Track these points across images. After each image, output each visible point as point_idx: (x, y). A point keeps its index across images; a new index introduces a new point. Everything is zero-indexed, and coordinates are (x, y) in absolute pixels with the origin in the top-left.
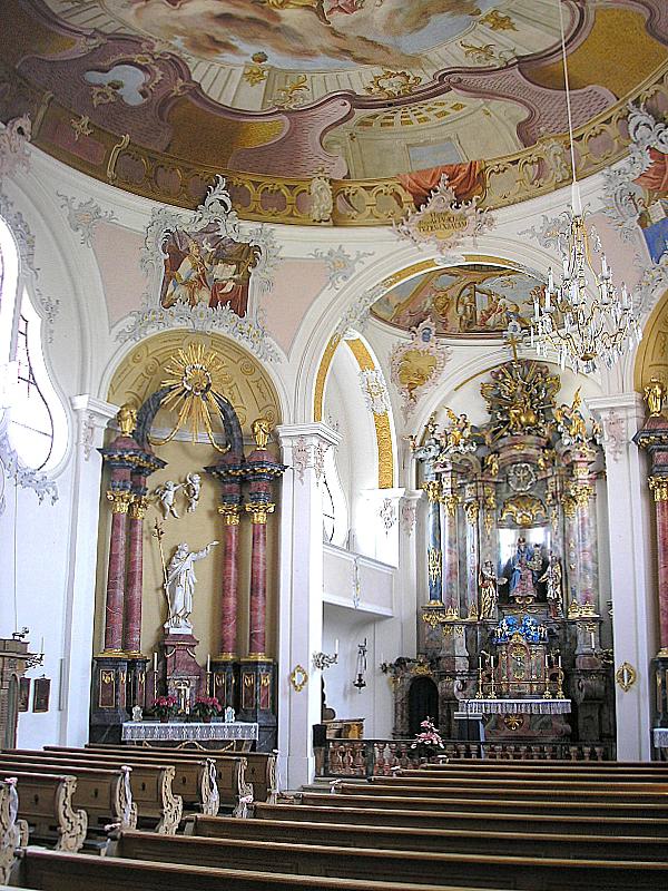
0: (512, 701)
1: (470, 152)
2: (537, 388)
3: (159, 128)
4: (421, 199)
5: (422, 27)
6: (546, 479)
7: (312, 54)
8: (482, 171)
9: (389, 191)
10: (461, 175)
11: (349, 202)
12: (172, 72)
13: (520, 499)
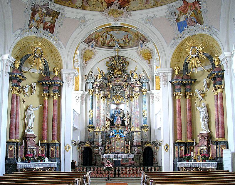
0: (117, 154)
2: (122, 64)
6: (125, 91)
11: (87, 3)
13: (117, 96)
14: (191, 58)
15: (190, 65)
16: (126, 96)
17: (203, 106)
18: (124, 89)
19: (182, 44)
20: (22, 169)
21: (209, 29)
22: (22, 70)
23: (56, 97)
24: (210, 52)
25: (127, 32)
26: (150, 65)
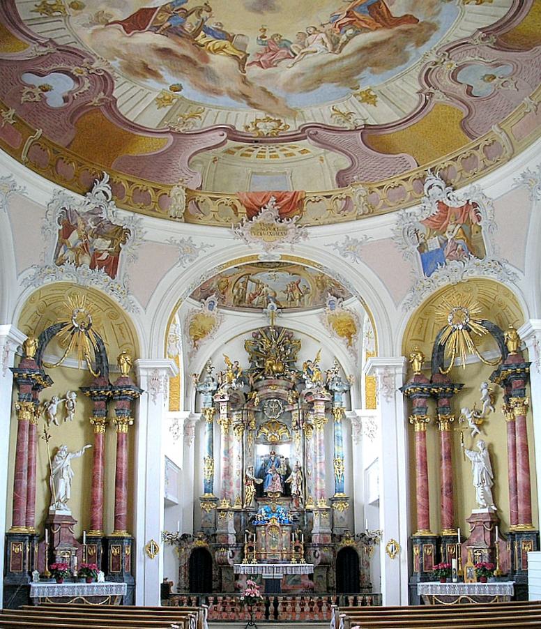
0: (272, 565)
1: (298, 185)
2: (285, 347)
3: (66, 127)
4: (253, 212)
5: (312, 90)
6: (290, 411)
7: (217, 93)
8: (301, 200)
9: (229, 203)
10: (286, 200)
11: (198, 207)
12: (99, 86)
13: (273, 425)
14: (451, 333)
15: (449, 350)
16: (294, 423)
17: (481, 449)
18: (288, 408)
19: (431, 301)
20: (43, 599)
21: (498, 267)
22: (42, 362)
23: (124, 425)
24: (497, 318)
25: (299, 275)
26: (353, 348)
